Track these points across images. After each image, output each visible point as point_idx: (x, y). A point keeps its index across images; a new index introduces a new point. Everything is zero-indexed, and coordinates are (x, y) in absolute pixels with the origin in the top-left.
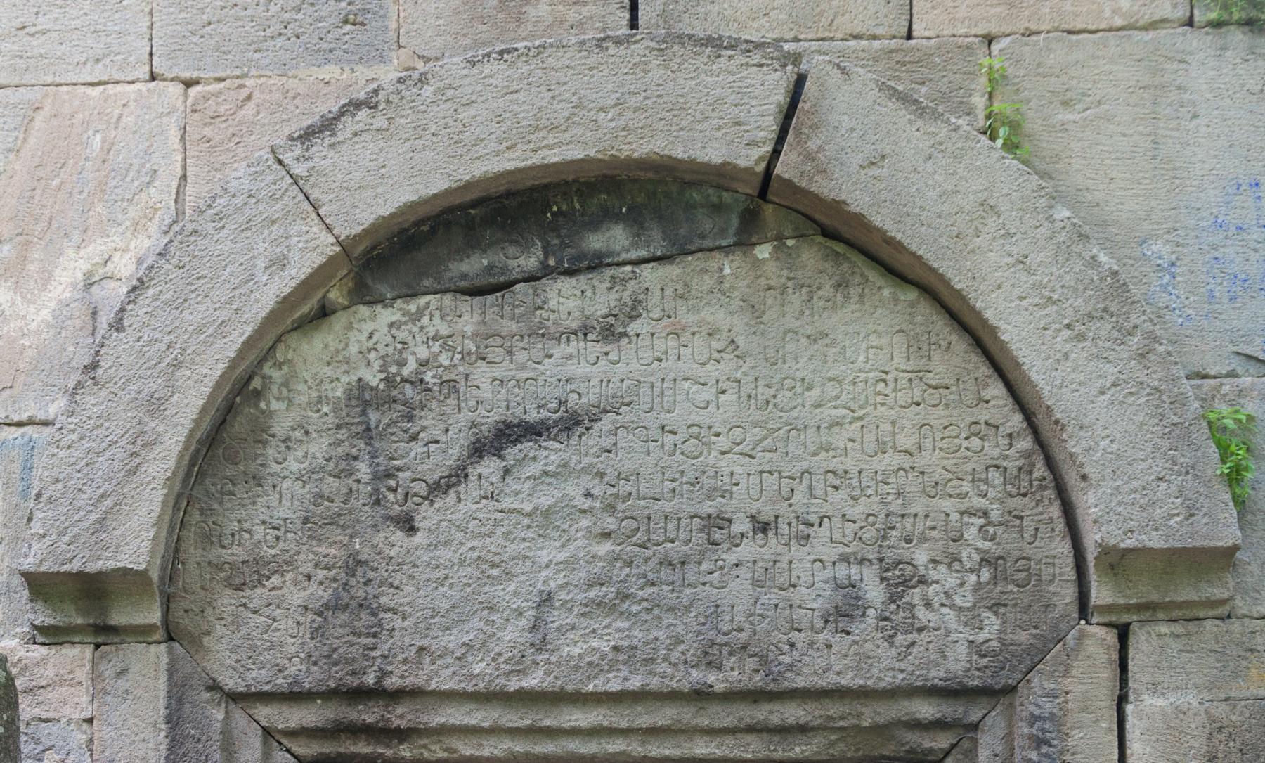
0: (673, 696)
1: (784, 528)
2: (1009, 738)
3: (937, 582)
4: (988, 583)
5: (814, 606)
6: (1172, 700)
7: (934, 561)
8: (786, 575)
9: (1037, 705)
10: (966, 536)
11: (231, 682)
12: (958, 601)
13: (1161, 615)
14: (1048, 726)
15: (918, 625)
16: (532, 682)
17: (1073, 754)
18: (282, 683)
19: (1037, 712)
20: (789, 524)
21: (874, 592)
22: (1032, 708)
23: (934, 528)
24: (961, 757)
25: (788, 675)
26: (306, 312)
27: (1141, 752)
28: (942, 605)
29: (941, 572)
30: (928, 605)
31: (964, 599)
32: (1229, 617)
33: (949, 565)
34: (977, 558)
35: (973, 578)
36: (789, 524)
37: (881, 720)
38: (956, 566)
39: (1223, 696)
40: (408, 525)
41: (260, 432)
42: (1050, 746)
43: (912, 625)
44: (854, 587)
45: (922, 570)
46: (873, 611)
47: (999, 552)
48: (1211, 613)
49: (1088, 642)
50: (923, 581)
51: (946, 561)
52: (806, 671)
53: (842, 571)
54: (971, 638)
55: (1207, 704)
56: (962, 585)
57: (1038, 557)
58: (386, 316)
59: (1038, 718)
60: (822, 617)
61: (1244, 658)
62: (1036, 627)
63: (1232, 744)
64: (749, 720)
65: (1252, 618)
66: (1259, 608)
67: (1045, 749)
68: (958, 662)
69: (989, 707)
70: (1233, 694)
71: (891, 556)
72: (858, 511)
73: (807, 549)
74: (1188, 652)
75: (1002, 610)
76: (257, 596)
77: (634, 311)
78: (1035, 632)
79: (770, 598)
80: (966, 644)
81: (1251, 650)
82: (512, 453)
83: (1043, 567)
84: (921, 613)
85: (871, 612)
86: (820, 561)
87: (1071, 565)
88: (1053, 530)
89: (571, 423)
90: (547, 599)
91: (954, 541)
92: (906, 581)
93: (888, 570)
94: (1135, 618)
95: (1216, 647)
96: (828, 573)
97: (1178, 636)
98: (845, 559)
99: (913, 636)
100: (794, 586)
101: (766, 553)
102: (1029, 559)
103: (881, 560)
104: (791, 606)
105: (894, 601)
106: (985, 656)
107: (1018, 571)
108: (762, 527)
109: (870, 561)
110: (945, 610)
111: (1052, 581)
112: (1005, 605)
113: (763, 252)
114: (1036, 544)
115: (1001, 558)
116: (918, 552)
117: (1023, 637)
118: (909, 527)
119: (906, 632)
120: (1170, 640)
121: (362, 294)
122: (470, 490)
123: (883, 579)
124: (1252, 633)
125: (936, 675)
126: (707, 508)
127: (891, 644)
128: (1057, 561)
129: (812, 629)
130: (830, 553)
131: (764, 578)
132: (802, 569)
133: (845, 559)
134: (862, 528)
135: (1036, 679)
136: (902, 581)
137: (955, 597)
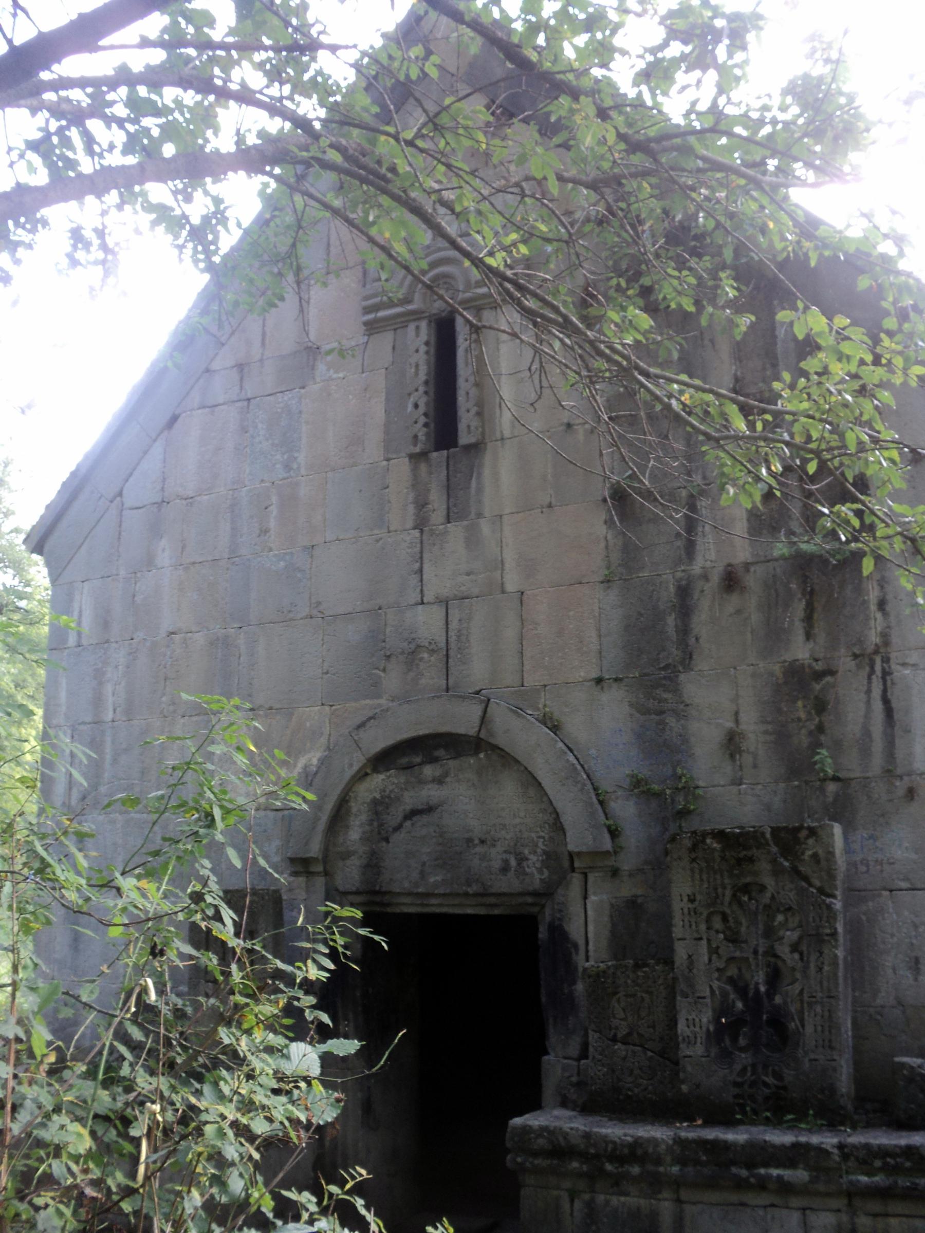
0: (458, 895)
11: (341, 889)
16: (420, 890)
18: (354, 889)
21: (513, 863)
26: (361, 776)
31: (538, 865)
40: (387, 840)
41: (348, 812)
50: (527, 859)
58: (382, 776)
72: (508, 837)
76: (348, 862)
77: (446, 774)
79: (484, 865)
82: (415, 819)
89: (429, 809)
90: (424, 864)
108: (482, 842)
113: (482, 755)
121: (376, 770)
122: (403, 831)
126: (466, 836)
131: (483, 858)
133: (505, 852)
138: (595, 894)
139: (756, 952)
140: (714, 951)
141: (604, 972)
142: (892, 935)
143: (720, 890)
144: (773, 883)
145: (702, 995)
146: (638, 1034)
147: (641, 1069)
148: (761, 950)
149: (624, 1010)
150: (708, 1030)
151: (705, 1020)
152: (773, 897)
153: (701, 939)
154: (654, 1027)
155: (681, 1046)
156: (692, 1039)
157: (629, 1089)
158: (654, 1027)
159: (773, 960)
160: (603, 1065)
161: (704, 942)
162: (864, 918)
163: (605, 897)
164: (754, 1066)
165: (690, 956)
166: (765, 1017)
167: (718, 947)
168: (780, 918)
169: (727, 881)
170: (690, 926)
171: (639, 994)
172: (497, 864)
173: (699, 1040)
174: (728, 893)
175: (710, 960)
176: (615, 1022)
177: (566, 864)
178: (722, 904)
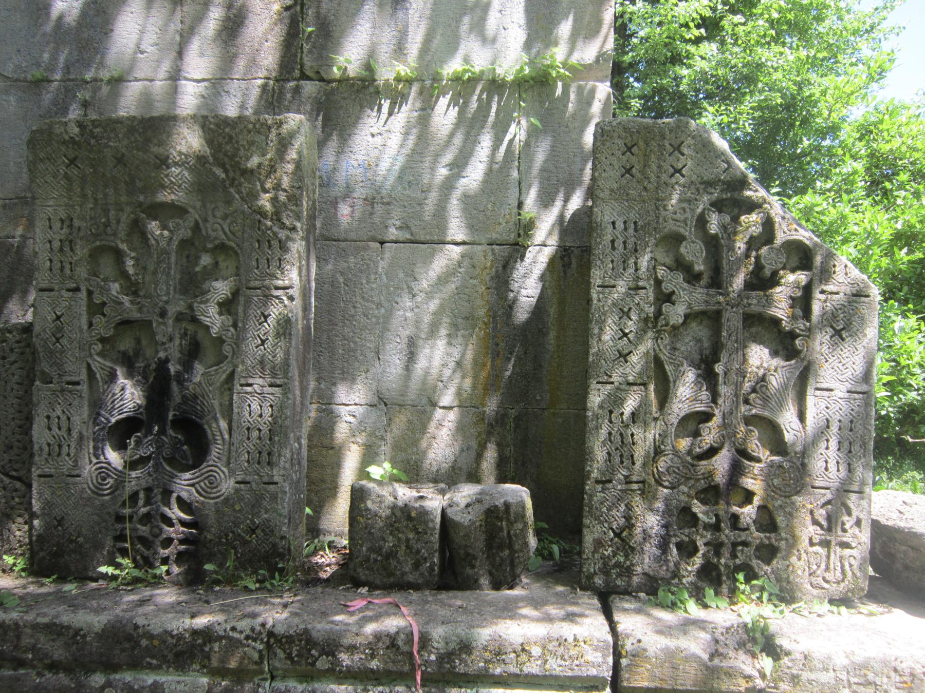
139: (163, 314)
140: (96, 309)
142: (379, 305)
143: (112, 213)
144: (198, 204)
145: (76, 379)
148: (172, 310)
150: (81, 433)
151: (76, 419)
152: (196, 228)
153: (77, 289)
155: (36, 458)
159: (191, 328)
161: (83, 294)
162: (341, 280)
164: (148, 490)
166: (170, 417)
167: (104, 304)
168: (206, 260)
169: (124, 199)
170: (62, 269)
173: (65, 449)
174: (125, 218)
175: (91, 325)
178: (115, 234)
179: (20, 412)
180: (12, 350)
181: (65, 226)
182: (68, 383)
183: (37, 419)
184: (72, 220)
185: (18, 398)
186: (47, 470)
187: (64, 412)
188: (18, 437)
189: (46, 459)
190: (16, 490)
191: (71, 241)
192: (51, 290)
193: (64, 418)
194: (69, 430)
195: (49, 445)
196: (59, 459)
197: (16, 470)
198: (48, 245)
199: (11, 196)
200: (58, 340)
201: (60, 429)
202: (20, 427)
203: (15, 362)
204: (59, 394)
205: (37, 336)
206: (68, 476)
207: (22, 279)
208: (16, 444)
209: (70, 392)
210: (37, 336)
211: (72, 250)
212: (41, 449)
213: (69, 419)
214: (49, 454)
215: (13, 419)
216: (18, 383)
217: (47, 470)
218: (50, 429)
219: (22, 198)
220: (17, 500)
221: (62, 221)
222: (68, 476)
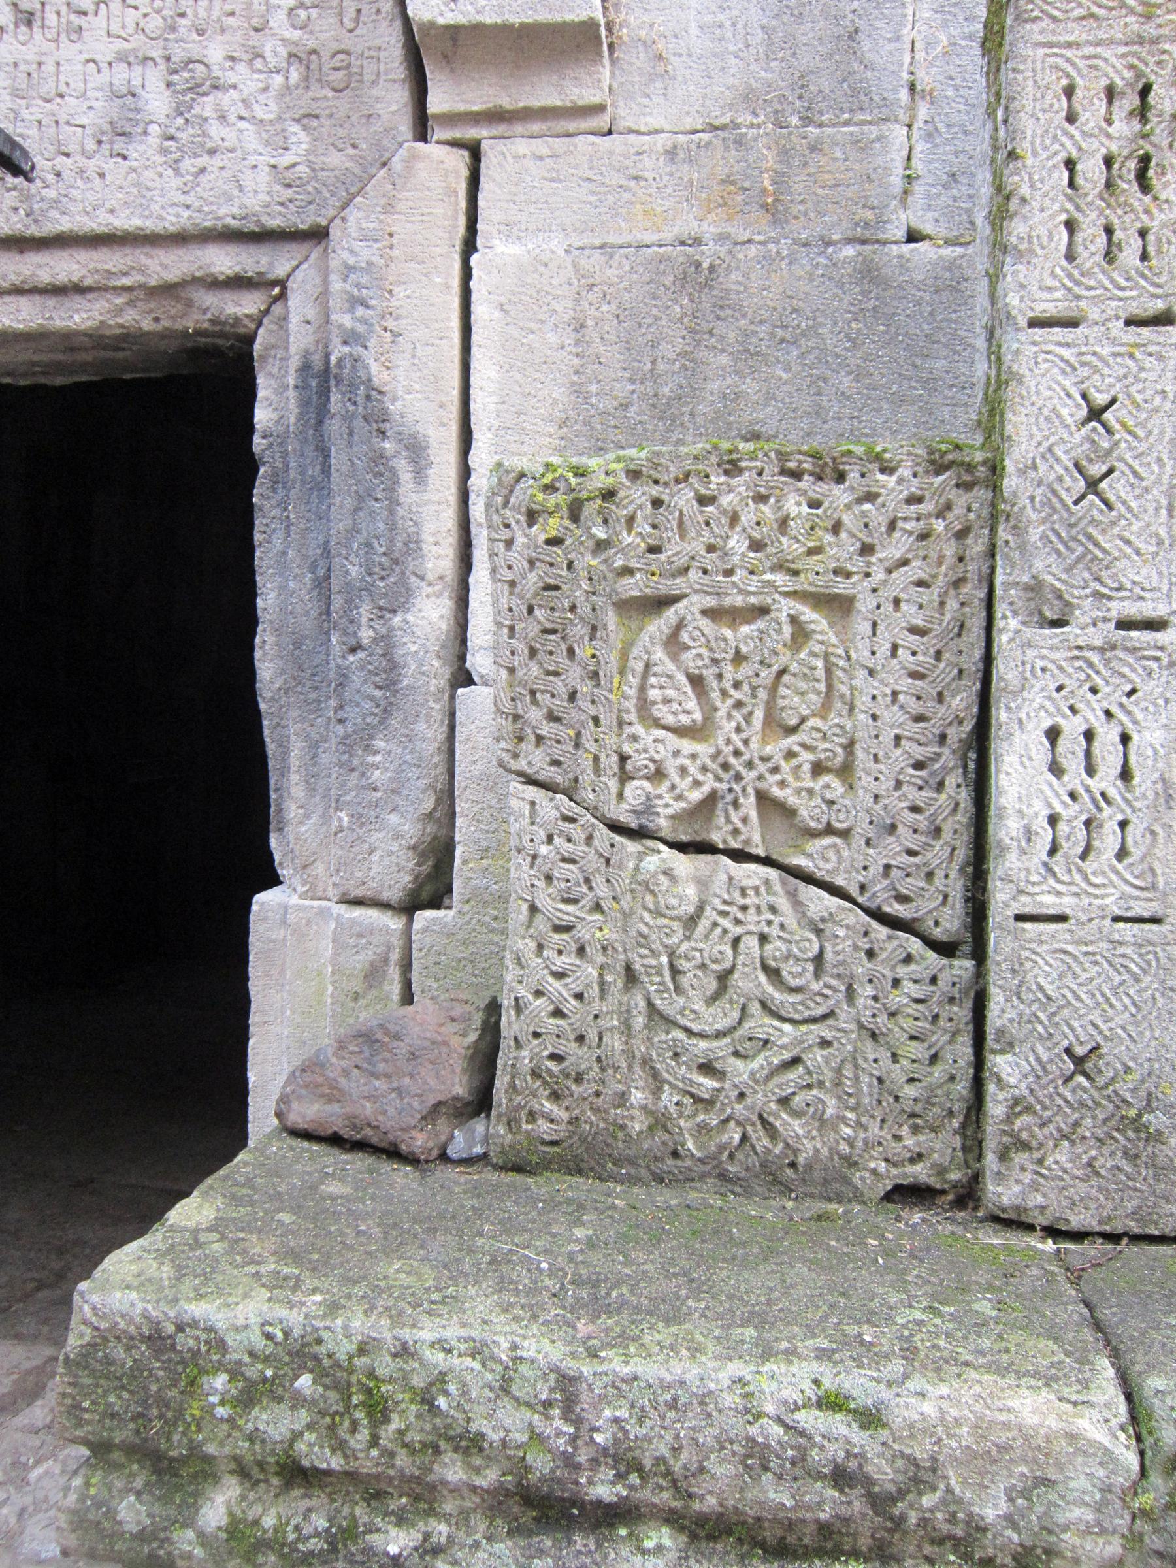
1: (52, 20)
2: (323, 298)
3: (234, 87)
4: (297, 87)
5: (83, 120)
6: (530, 246)
7: (232, 59)
8: (52, 82)
9: (352, 252)
10: (271, 24)
12: (259, 111)
13: (519, 129)
14: (364, 280)
15: (210, 145)
17: (396, 319)
19: (351, 261)
20: (58, 13)
21: (157, 102)
22: (345, 255)
23: (232, 14)
24: (275, 327)
25: (53, 214)
27: (487, 317)
28: (241, 118)
29: (240, 74)
30: (222, 118)
32: (610, 133)
33: (250, 62)
34: (283, 52)
35: (278, 79)
36: (58, 13)
37: (172, 276)
38: (258, 64)
39: (598, 242)
42: (368, 307)
43: (202, 145)
44: (134, 95)
45: (216, 71)
46: (156, 127)
47: (312, 44)
48: (584, 124)
49: (420, 165)
51: (245, 57)
52: (73, 208)
53: (121, 76)
54: (273, 161)
55: (576, 253)
56: (265, 89)
57: (359, 49)
59: (351, 269)
60: (94, 136)
61: (627, 189)
62: (354, 146)
63: (605, 308)
64: (13, 277)
65: (638, 133)
66: (649, 119)
67: (360, 311)
68: (255, 197)
69: (299, 257)
70: (611, 239)
71: (179, 53)
73: (77, 46)
74: (553, 180)
75: (315, 123)
78: (351, 151)
80: (267, 169)
81: (636, 178)
83: (365, 62)
84: (215, 130)
85: (154, 129)
86: (94, 61)
87: (400, 59)
88: (378, 11)
91: (257, 30)
92: (198, 86)
93: (176, 72)
94: (484, 133)
95: (590, 174)
96: (105, 77)
97: (541, 158)
98: (123, 58)
99: (204, 160)
100: (62, 96)
101: (28, 54)
102: (348, 53)
103: (168, 59)
104: (57, 122)
105: (182, 114)
106: (289, 186)
107: (335, 69)
109: (152, 59)
110: (243, 125)
111: (374, 83)
112: (317, 117)
114: (358, 32)
115: (314, 52)
116: (211, 46)
117: (335, 159)
118: (202, 13)
119: (196, 155)
120: (531, 164)
123: (169, 85)
124: (639, 154)
125: (227, 214)
127: (177, 172)
128: (382, 54)
129: (83, 152)
130: (105, 50)
132: (73, 72)
134: (145, 15)
135: (353, 215)
136: (193, 85)
137: (256, 107)
138: (509, 229)
141: (609, 495)
146: (763, 798)
147: (773, 974)
149: (696, 681)
154: (845, 771)
156: (1073, 835)
157: (707, 1068)
158: (845, 771)
160: (581, 951)
163: (556, 244)
165: (1096, 414)
171: (785, 608)
172: (90, 112)
173: (1109, 840)
176: (650, 745)
177: (394, 100)
179: (919, 718)
180: (892, 526)
181: (1118, 113)
182: (1124, 624)
183: (1018, 738)
184: (1145, 91)
185: (915, 675)
186: (1049, 899)
187: (1108, 714)
188: (914, 795)
189: (1045, 865)
190: (908, 959)
191: (1145, 160)
192: (1072, 323)
193: (1108, 736)
194: (1126, 775)
195: (1053, 820)
196: (1089, 866)
197: (903, 899)
198: (1066, 174)
199: (688, 123)
200: (1093, 485)
201: (1090, 770)
202: (919, 765)
203: (905, 562)
204: (1094, 657)
205: (1022, 472)
206: (1116, 919)
207: (724, 359)
208: (909, 816)
209: (1134, 650)
210: (1022, 472)
211: (1144, 185)
212: (1029, 834)
213: (1125, 739)
214: (1053, 850)
215: (898, 738)
216: (914, 630)
217: (1049, 899)
218: (1056, 769)
219: (723, 128)
220: (909, 987)
221: (1111, 93)
222: (1116, 919)
